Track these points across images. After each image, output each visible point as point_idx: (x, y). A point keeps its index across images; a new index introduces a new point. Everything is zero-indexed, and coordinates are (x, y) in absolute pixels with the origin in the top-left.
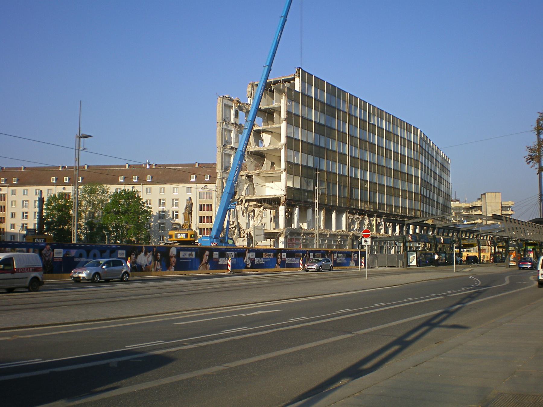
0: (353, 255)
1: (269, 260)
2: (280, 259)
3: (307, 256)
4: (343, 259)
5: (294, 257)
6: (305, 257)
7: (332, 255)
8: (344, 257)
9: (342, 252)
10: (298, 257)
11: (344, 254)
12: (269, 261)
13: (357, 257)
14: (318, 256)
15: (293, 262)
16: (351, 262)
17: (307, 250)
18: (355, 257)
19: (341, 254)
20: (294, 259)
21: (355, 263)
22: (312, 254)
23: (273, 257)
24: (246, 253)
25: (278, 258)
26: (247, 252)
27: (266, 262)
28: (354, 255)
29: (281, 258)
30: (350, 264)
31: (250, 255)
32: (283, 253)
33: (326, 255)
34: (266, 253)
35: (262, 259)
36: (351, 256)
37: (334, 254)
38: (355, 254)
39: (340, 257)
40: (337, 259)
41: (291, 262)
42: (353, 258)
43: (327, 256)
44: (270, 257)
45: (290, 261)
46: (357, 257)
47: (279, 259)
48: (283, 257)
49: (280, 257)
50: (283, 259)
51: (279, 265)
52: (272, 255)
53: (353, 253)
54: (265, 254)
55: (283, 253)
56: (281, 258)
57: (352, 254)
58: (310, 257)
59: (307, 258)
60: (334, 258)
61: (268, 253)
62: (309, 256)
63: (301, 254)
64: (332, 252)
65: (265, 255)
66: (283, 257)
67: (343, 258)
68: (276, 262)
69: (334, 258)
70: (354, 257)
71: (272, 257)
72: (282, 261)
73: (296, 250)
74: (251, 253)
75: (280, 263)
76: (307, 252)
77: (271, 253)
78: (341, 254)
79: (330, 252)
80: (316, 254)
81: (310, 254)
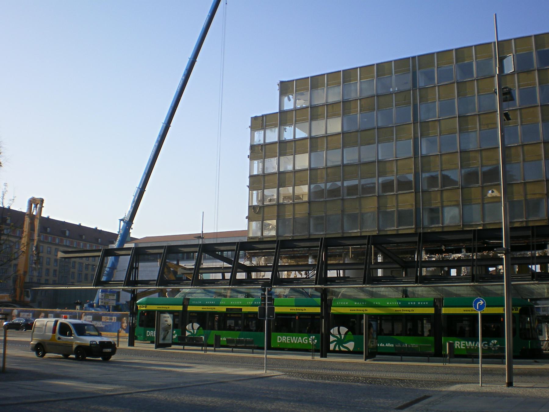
1: (111, 324)
12: (110, 325)
23: (116, 321)
24: (82, 316)
26: (83, 315)
27: (106, 326)
31: (86, 318)
34: (106, 317)
35: (101, 322)
47: (124, 323)
49: (125, 322)
51: (124, 330)
54: (105, 318)
61: (109, 317)
65: (105, 319)
68: (120, 326)
74: (87, 316)
75: (125, 328)
77: (113, 318)
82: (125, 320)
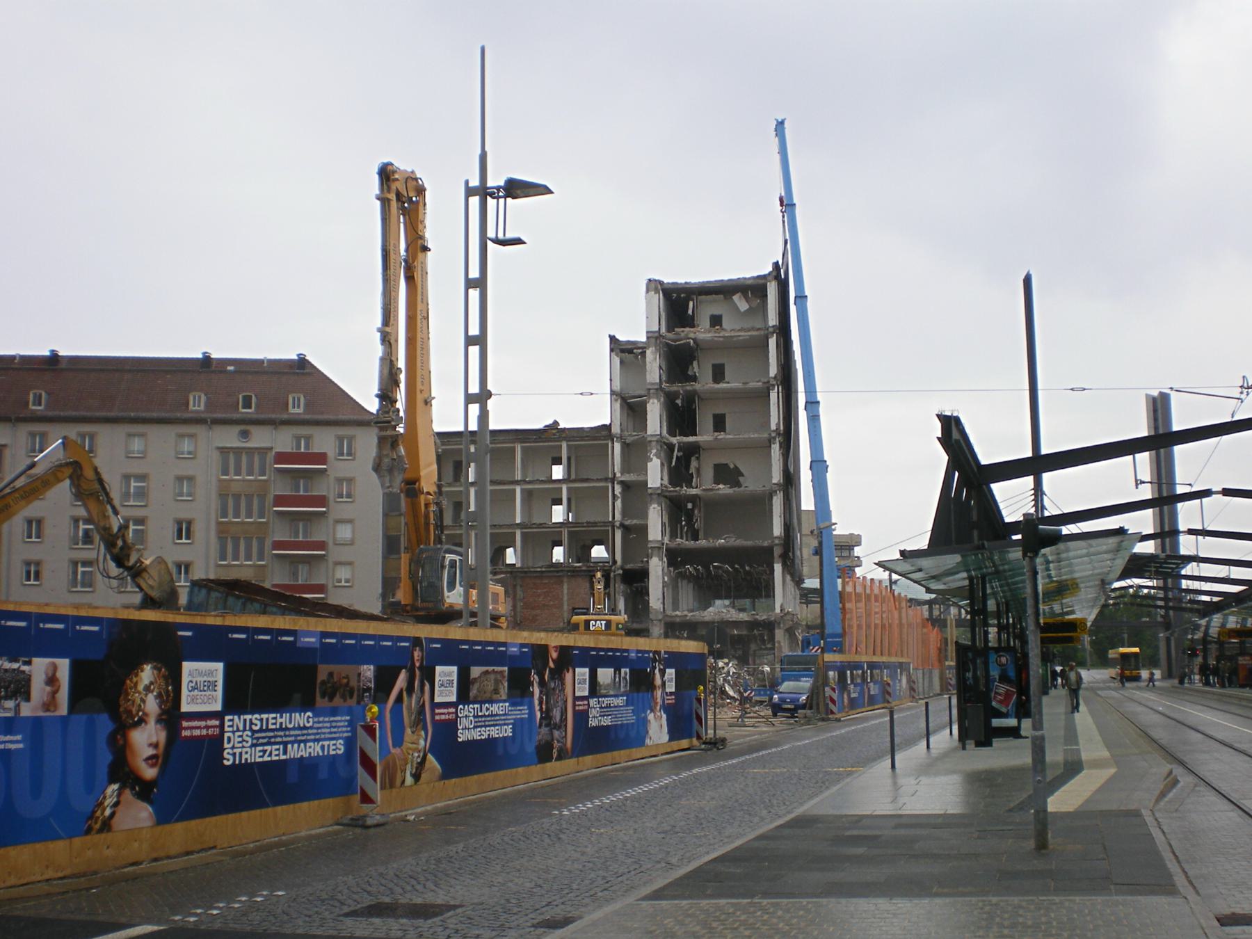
0: (658, 681)
2: (152, 721)
3: (410, 689)
4: (621, 701)
5: (307, 704)
6: (399, 699)
7: (569, 676)
8: (622, 690)
9: (614, 659)
10: (337, 700)
11: (623, 670)
13: (673, 690)
14: (490, 686)
15: (294, 752)
16: (651, 716)
17: (416, 642)
18: (668, 690)
19: (612, 670)
20: (301, 719)
21: (667, 720)
22: (446, 674)
23: (63, 710)
25: (124, 722)
28: (663, 673)
29: (171, 716)
30: (647, 732)
32: (187, 666)
33: (535, 678)
36: (651, 687)
37: (578, 670)
38: (667, 670)
39: (603, 692)
40: (593, 702)
41: (274, 754)
42: (659, 693)
43: (542, 683)
44: (27, 710)
45: (262, 737)
46: (673, 690)
47: (142, 721)
48: (185, 707)
49: (152, 705)
50: (191, 730)
51: (145, 791)
52: (52, 680)
53: (660, 663)
55: (187, 666)
56: (171, 716)
57: (657, 671)
58: (437, 699)
59: (410, 703)
60: (576, 699)
62: (427, 687)
63: (368, 671)
64: (568, 658)
66: (185, 707)
67: (616, 696)
69: (576, 699)
70: (664, 684)
71: (50, 704)
72: (168, 756)
73: (325, 635)
75: (150, 773)
76: (417, 654)
77: (39, 667)
78: (612, 670)
79: (554, 655)
80: (476, 671)
81: (439, 669)
82: (148, 689)
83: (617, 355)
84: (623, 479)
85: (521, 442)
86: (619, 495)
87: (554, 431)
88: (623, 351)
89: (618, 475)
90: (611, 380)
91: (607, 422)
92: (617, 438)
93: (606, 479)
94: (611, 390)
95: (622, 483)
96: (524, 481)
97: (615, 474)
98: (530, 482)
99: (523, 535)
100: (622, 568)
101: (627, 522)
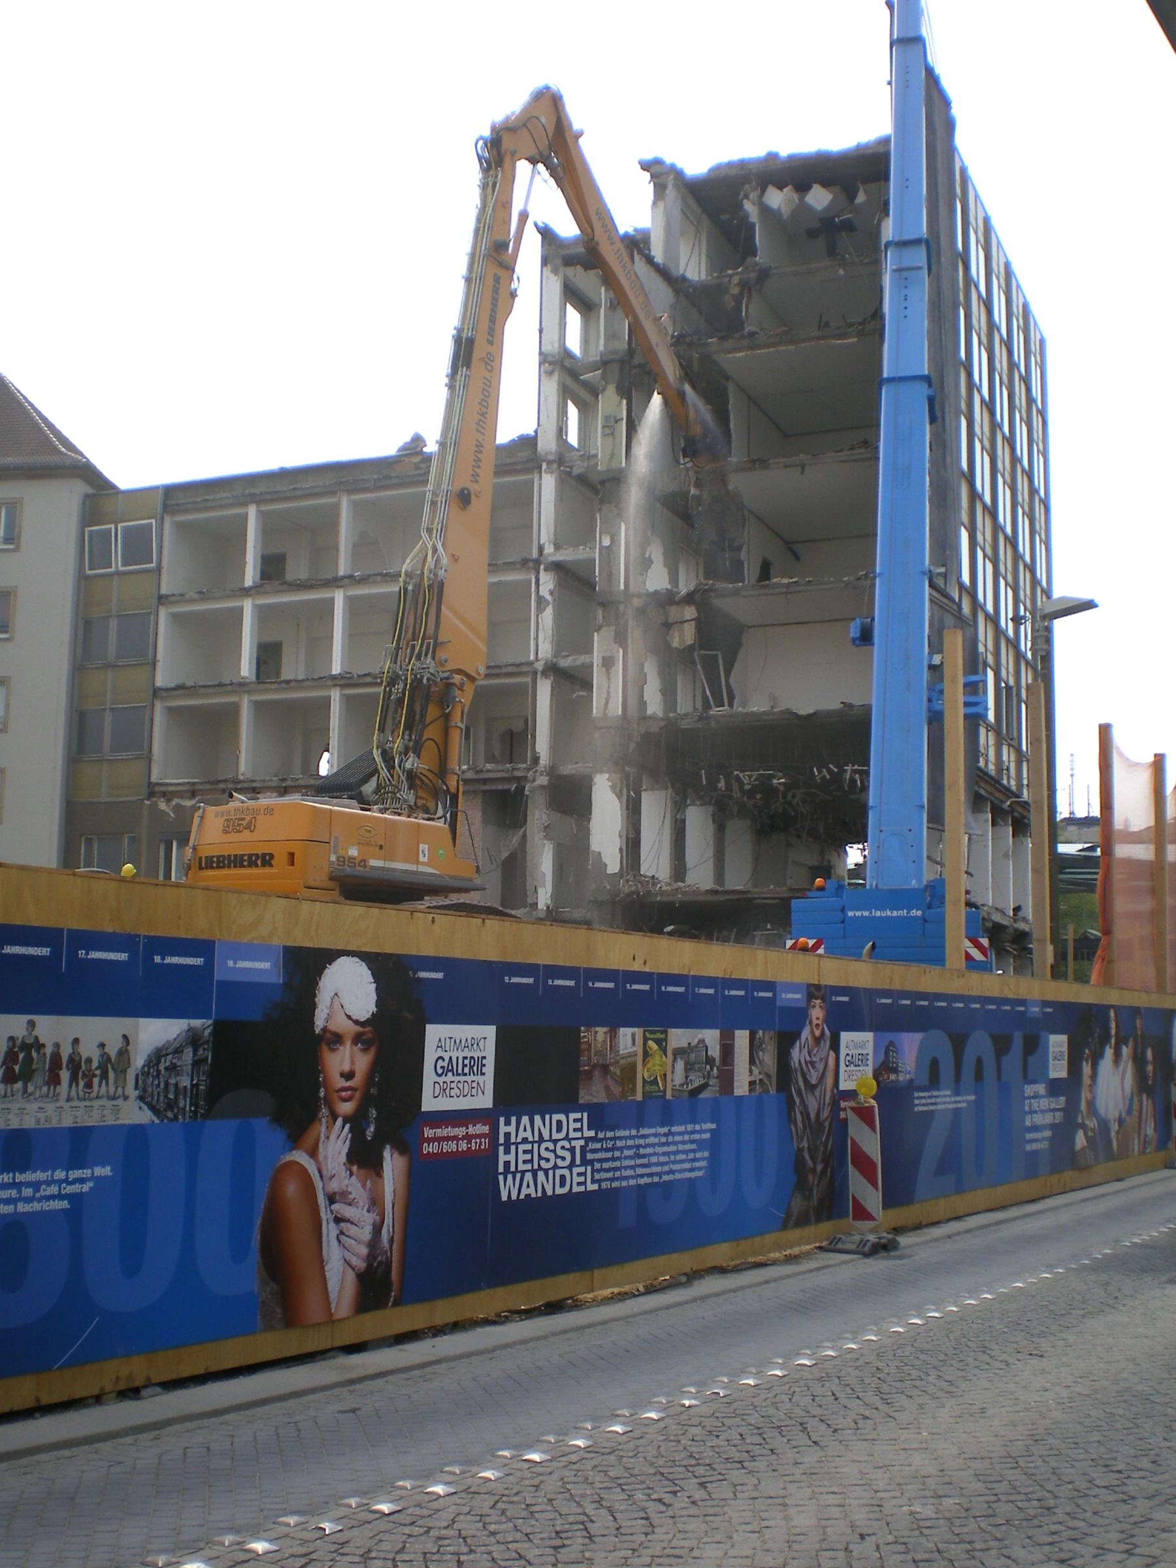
83: (555, 271)
84: (560, 557)
85: (350, 492)
86: (549, 598)
87: (416, 459)
88: (569, 261)
89: (549, 549)
90: (541, 331)
91: (529, 430)
92: (549, 463)
93: (525, 563)
94: (541, 353)
95: (558, 568)
96: (352, 580)
97: (541, 549)
98: (363, 581)
99: (348, 701)
100: (552, 771)
101: (564, 663)
